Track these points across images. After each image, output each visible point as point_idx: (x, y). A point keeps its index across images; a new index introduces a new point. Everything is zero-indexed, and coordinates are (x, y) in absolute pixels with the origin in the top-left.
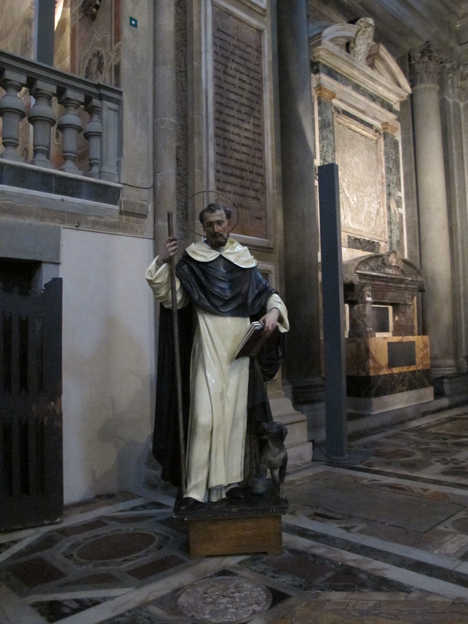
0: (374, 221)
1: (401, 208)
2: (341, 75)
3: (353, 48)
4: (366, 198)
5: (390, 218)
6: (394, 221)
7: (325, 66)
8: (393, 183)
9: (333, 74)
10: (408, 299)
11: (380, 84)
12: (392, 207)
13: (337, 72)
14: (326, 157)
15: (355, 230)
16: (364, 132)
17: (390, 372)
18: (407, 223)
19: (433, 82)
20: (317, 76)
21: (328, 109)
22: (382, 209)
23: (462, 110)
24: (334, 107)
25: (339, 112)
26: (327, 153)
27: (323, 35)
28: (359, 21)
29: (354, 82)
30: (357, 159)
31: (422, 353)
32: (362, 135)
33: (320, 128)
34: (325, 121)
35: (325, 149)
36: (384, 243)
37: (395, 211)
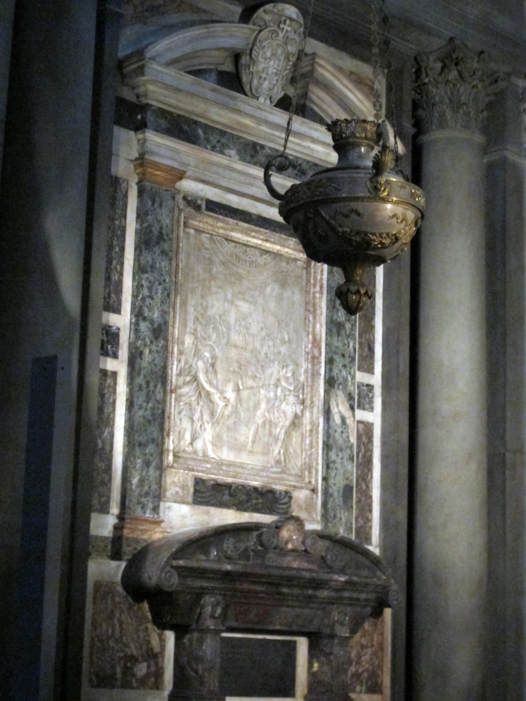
0: (280, 444)
2: (206, 128)
4: (263, 392)
5: (328, 435)
6: (340, 441)
7: (163, 113)
8: (343, 356)
9: (186, 127)
10: (342, 624)
11: (314, 140)
12: (334, 410)
13: (196, 123)
14: (146, 310)
15: (220, 464)
16: (268, 245)
18: (384, 444)
19: (466, 127)
20: (140, 136)
21: (161, 206)
22: (307, 414)
24: (185, 198)
25: (198, 208)
26: (148, 301)
27: (150, 53)
28: (261, 10)
29: (246, 139)
30: (244, 307)
32: (267, 252)
33: (138, 248)
34: (151, 232)
35: (145, 292)
36: (308, 492)
37: (343, 420)
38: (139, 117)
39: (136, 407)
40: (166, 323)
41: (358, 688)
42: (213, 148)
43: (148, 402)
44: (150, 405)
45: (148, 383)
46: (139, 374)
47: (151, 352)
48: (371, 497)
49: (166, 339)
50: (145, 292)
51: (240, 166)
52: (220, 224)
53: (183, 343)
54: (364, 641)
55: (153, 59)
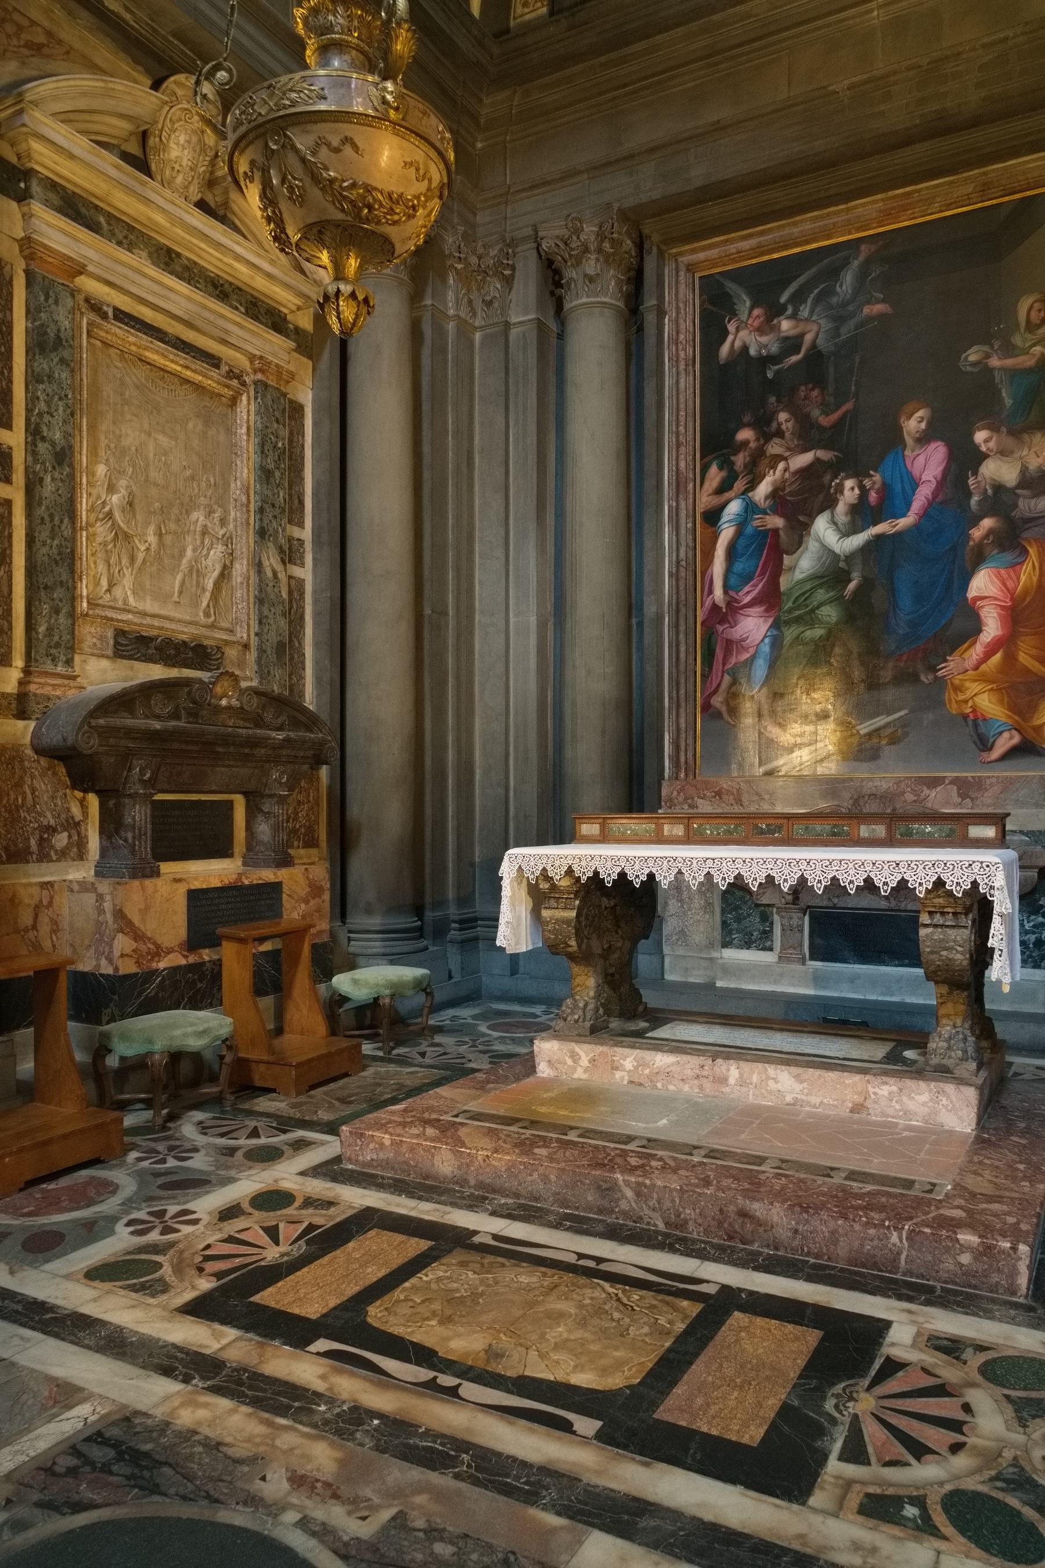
1: (302, 565)
3: (157, 151)
7: (53, 186)
8: (273, 505)
9: (83, 210)
12: (266, 563)
14: (45, 429)
17: (192, 959)
21: (56, 302)
23: (477, 350)
24: (87, 300)
25: (104, 316)
26: (47, 418)
29: (159, 242)
30: (164, 440)
31: (303, 906)
32: (187, 381)
34: (46, 333)
35: (42, 406)
37: (275, 574)
38: (22, 185)
39: (38, 544)
40: (71, 447)
41: (296, 843)
42: (119, 243)
43: (53, 539)
44: (56, 542)
45: (51, 516)
46: (40, 504)
47: (53, 479)
48: (304, 655)
49: (72, 466)
50: (42, 406)
51: (153, 271)
52: (132, 339)
53: (93, 474)
54: (300, 798)
55: (35, 104)
